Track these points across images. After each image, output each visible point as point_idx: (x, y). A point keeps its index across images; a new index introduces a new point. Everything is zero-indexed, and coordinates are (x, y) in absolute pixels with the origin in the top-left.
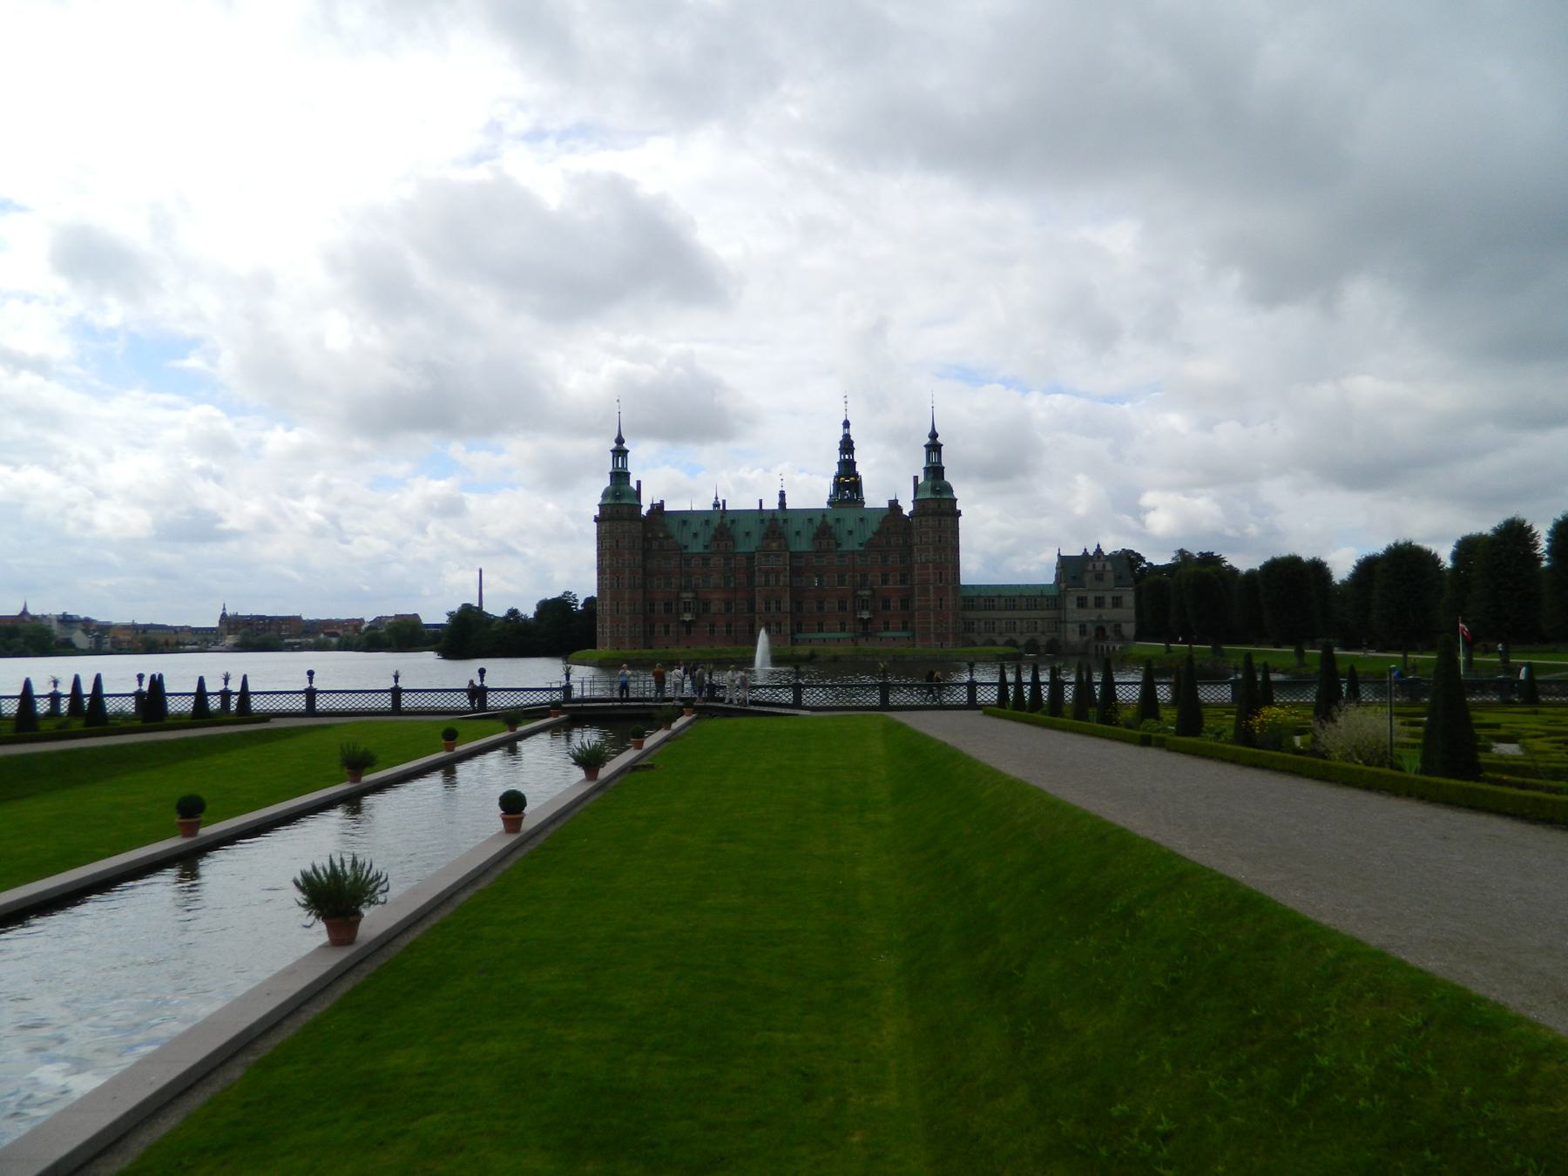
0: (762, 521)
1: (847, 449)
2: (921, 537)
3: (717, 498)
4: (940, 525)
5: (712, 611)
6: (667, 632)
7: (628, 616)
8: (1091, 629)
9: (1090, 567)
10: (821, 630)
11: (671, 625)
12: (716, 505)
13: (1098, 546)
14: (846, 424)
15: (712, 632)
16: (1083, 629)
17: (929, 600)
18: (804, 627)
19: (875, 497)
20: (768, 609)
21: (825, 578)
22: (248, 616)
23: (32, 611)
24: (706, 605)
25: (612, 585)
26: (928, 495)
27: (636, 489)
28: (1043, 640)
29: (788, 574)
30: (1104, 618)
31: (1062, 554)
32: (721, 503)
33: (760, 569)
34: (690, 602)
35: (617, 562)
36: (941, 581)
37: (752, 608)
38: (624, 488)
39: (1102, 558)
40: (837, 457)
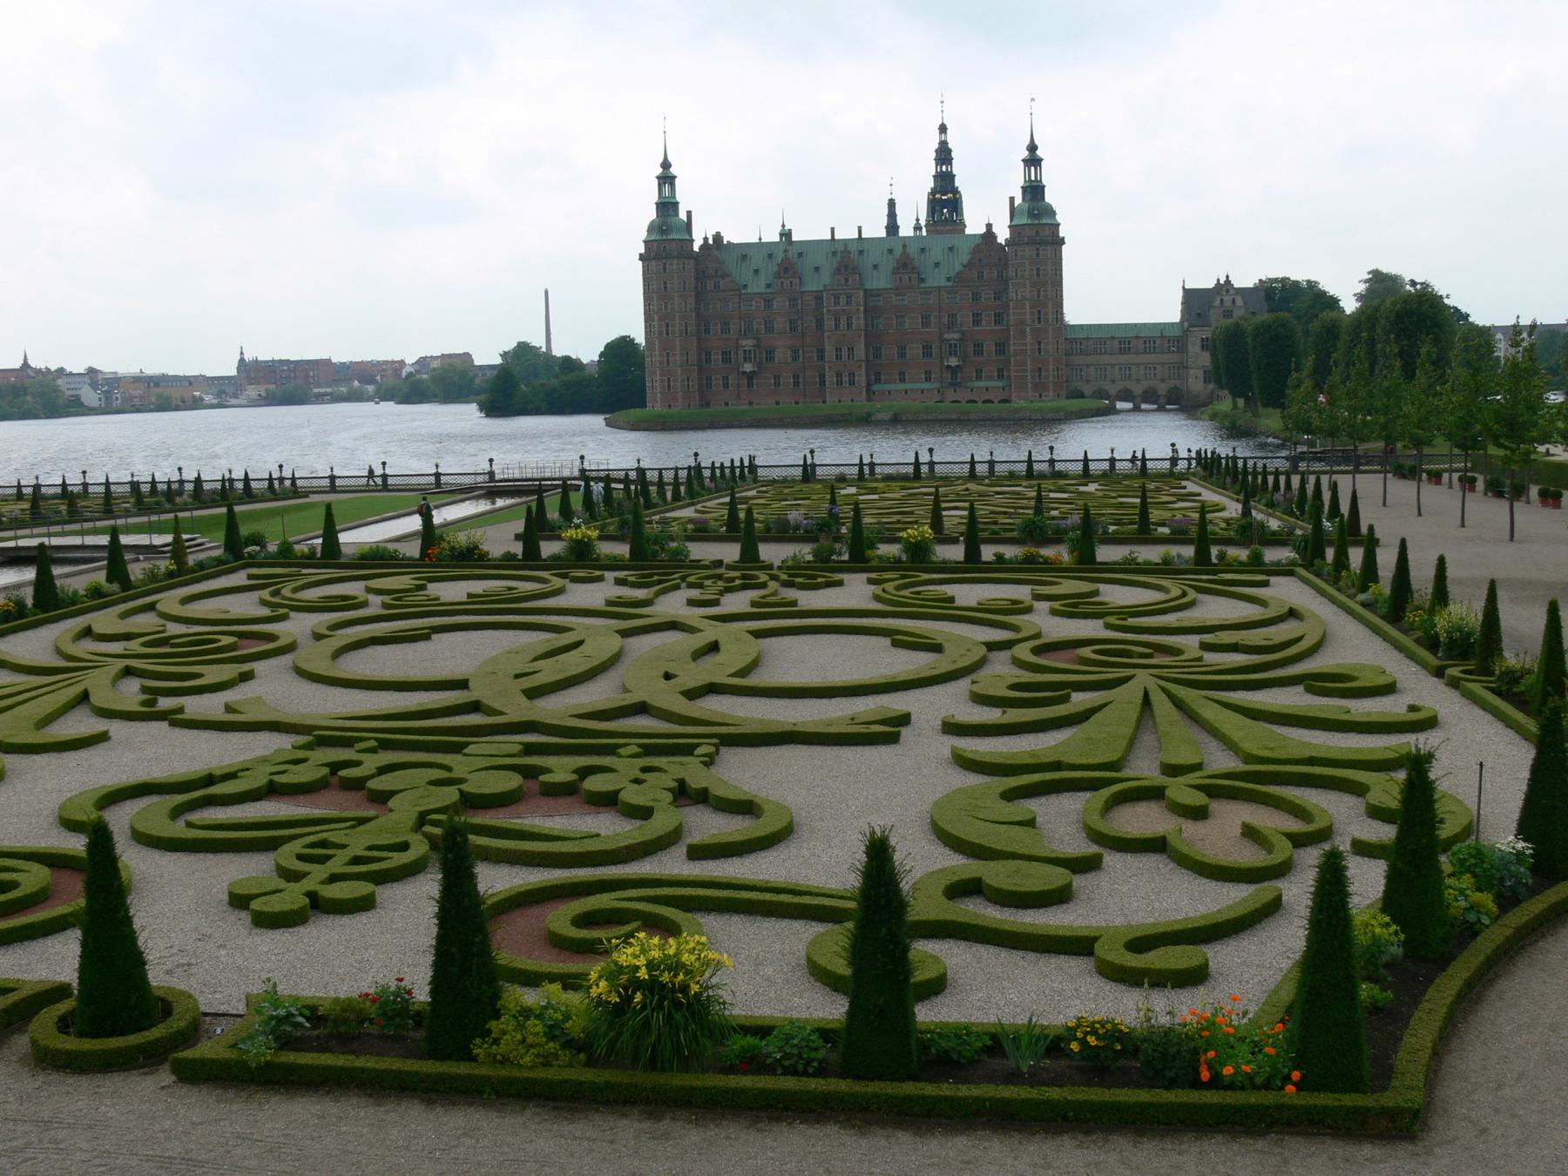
0: (834, 253)
1: (944, 159)
3: (783, 226)
4: (1038, 255)
6: (726, 385)
9: (1217, 303)
10: (903, 380)
13: (1227, 277)
14: (943, 129)
15: (777, 384)
17: (1025, 344)
18: (882, 377)
20: (839, 357)
22: (268, 362)
23: (36, 363)
25: (660, 333)
26: (1024, 220)
28: (1162, 389)
29: (862, 315)
31: (1186, 287)
33: (829, 311)
34: (750, 351)
35: (666, 307)
36: (1039, 322)
37: (821, 352)
39: (1232, 292)
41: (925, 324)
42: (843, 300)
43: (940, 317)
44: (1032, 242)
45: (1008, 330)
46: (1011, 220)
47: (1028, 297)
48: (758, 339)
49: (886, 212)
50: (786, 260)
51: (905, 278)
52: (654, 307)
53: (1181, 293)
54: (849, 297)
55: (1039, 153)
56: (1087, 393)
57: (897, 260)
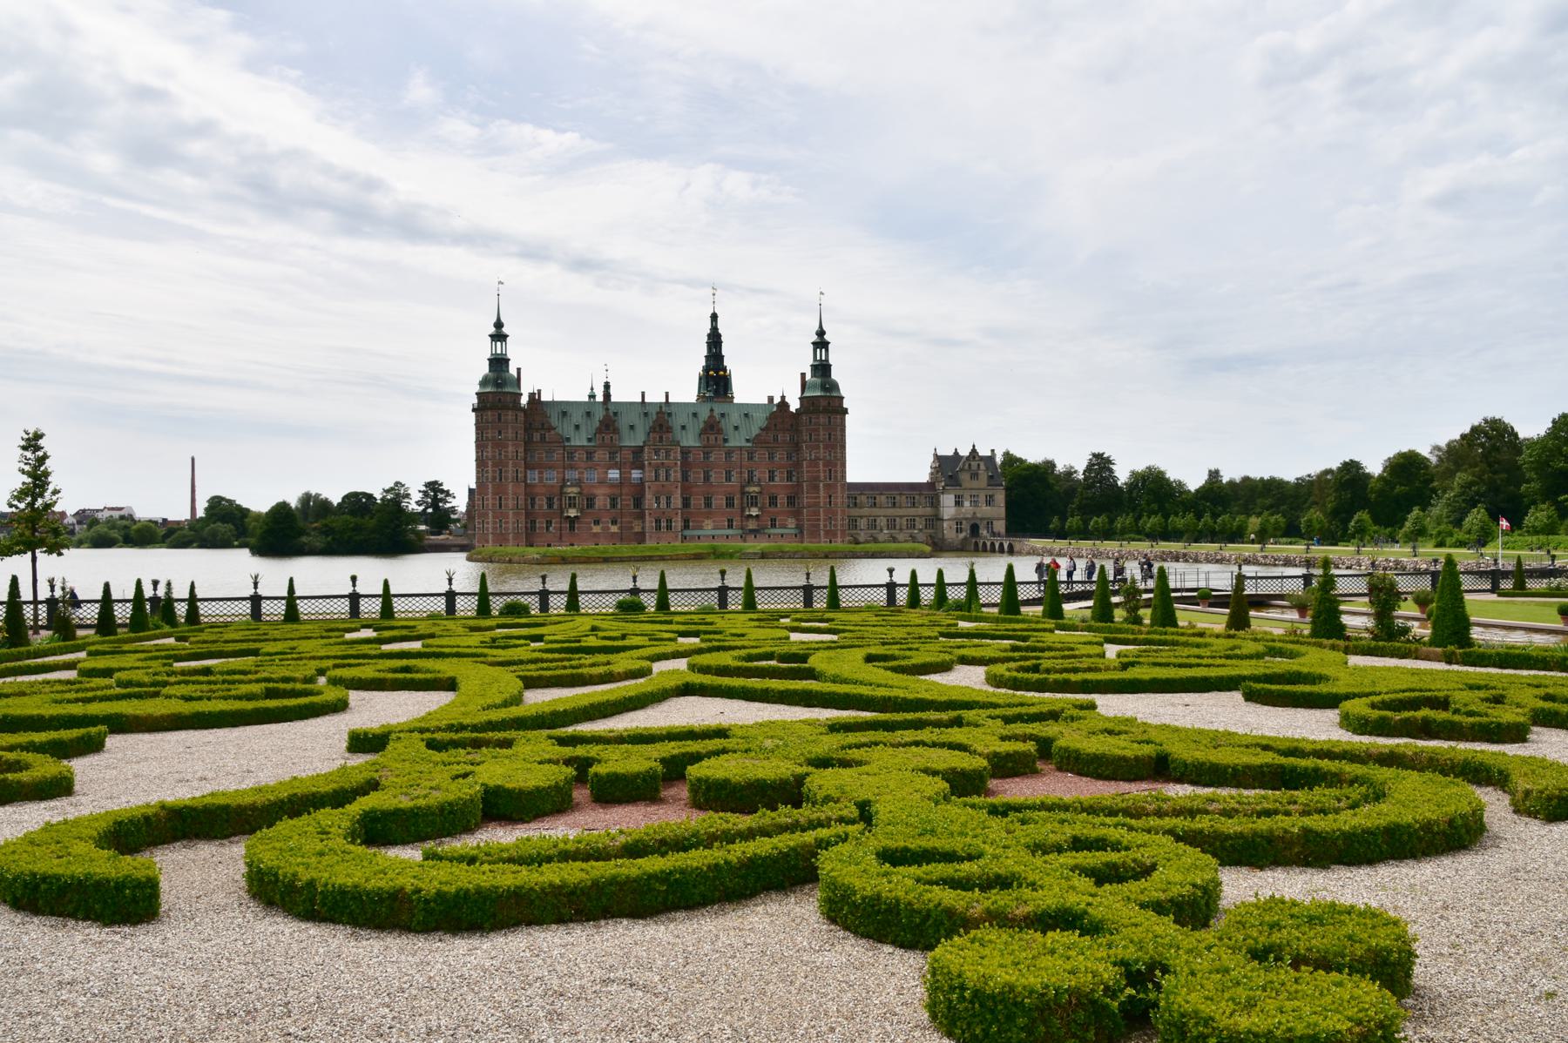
0: (646, 414)
2: (811, 435)
3: (592, 389)
4: (830, 422)
5: (596, 506)
7: (511, 512)
8: (966, 526)
11: (554, 521)
13: (974, 446)
14: (714, 317)
16: (959, 530)
21: (712, 473)
24: (591, 502)
27: (515, 375)
30: (979, 515)
33: (650, 464)
34: (574, 498)
35: (500, 454)
41: (728, 479)
42: (662, 454)
43: (741, 473)
44: (825, 411)
45: (799, 485)
48: (580, 487)
50: (607, 417)
51: (713, 437)
53: (930, 459)
55: (826, 337)
56: (880, 539)
57: (705, 422)
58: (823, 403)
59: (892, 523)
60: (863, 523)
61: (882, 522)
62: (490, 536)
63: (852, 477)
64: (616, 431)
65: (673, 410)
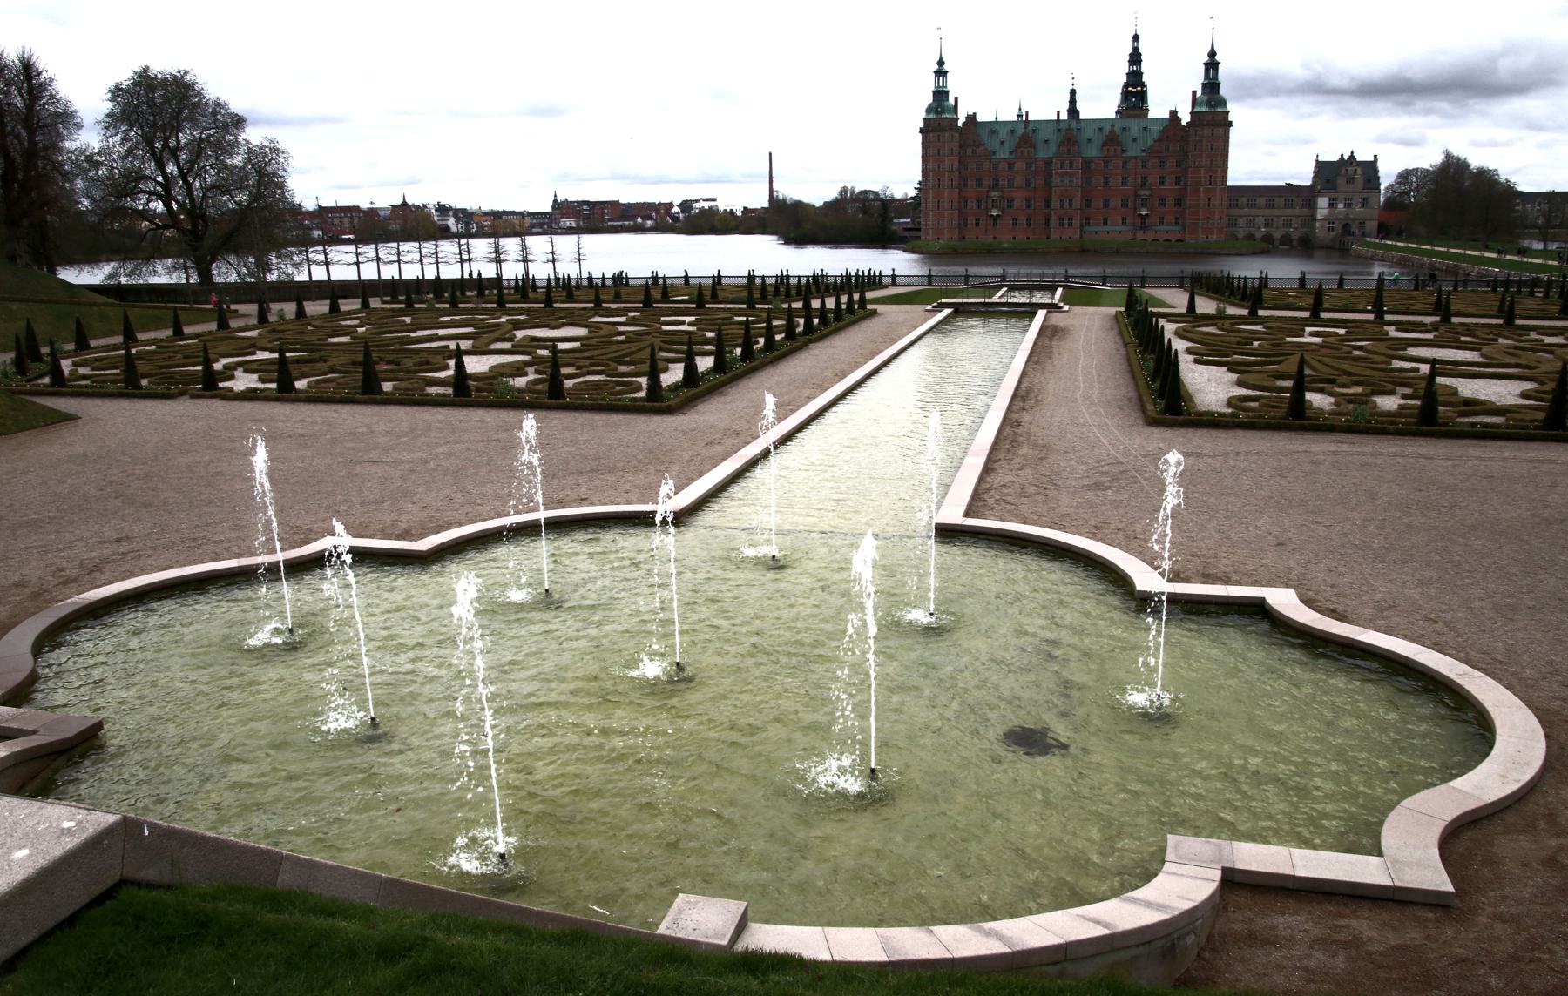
0: (1059, 130)
3: (1020, 109)
6: (977, 224)
9: (1343, 172)
10: (1105, 223)
12: (1020, 116)
13: (1352, 153)
14: (1136, 38)
15: (1015, 224)
19: (1158, 109)
20: (1062, 206)
23: (409, 202)
24: (1010, 203)
25: (934, 186)
26: (1204, 109)
28: (1296, 235)
32: (1024, 114)
37: (1048, 204)
38: (946, 103)
40: (1125, 68)
42: (1067, 164)
43: (1135, 178)
44: (1209, 124)
46: (1193, 107)
47: (1203, 164)
49: (1068, 99)
51: (1112, 149)
52: (930, 167)
53: (1314, 164)
54: (1071, 163)
55: (1217, 58)
58: (1209, 117)
59: (1269, 223)
60: (1242, 222)
61: (1260, 221)
62: (931, 231)
63: (1230, 183)
64: (1033, 146)
65: (1083, 124)
